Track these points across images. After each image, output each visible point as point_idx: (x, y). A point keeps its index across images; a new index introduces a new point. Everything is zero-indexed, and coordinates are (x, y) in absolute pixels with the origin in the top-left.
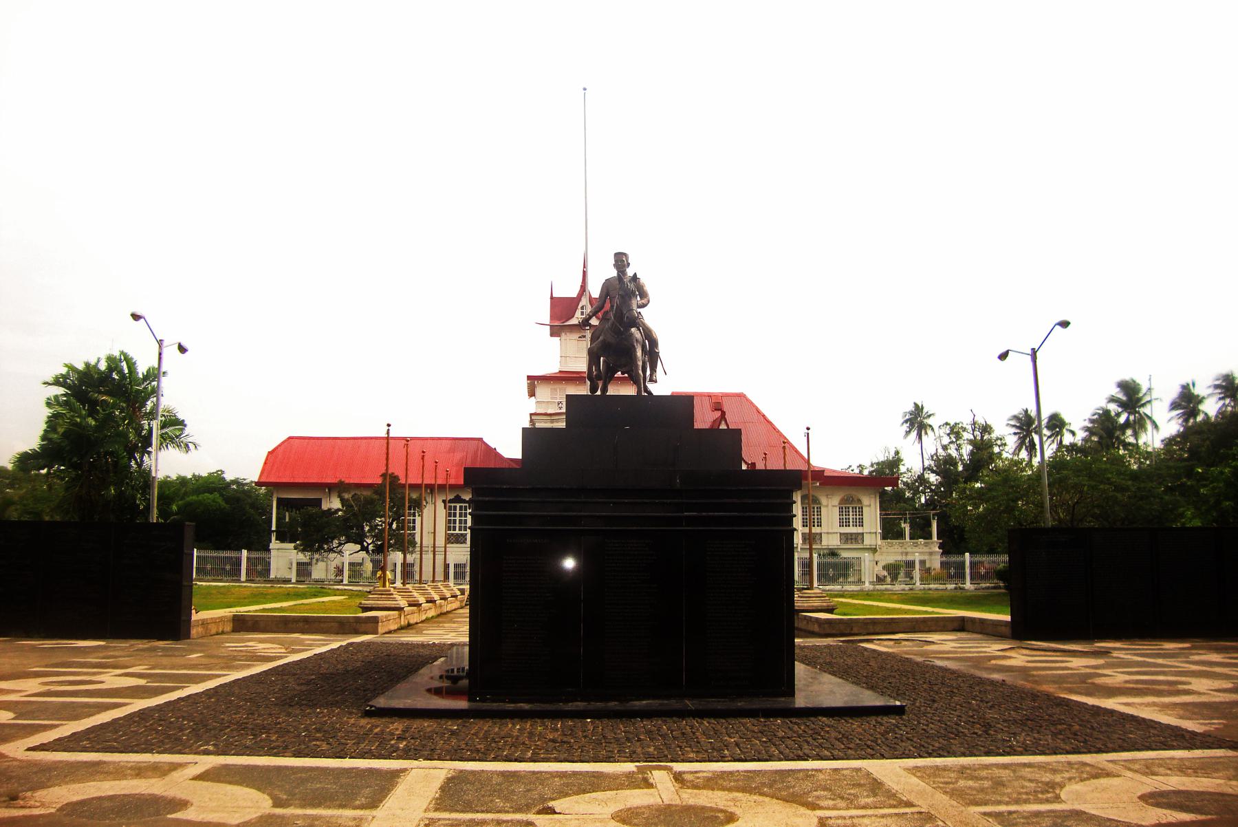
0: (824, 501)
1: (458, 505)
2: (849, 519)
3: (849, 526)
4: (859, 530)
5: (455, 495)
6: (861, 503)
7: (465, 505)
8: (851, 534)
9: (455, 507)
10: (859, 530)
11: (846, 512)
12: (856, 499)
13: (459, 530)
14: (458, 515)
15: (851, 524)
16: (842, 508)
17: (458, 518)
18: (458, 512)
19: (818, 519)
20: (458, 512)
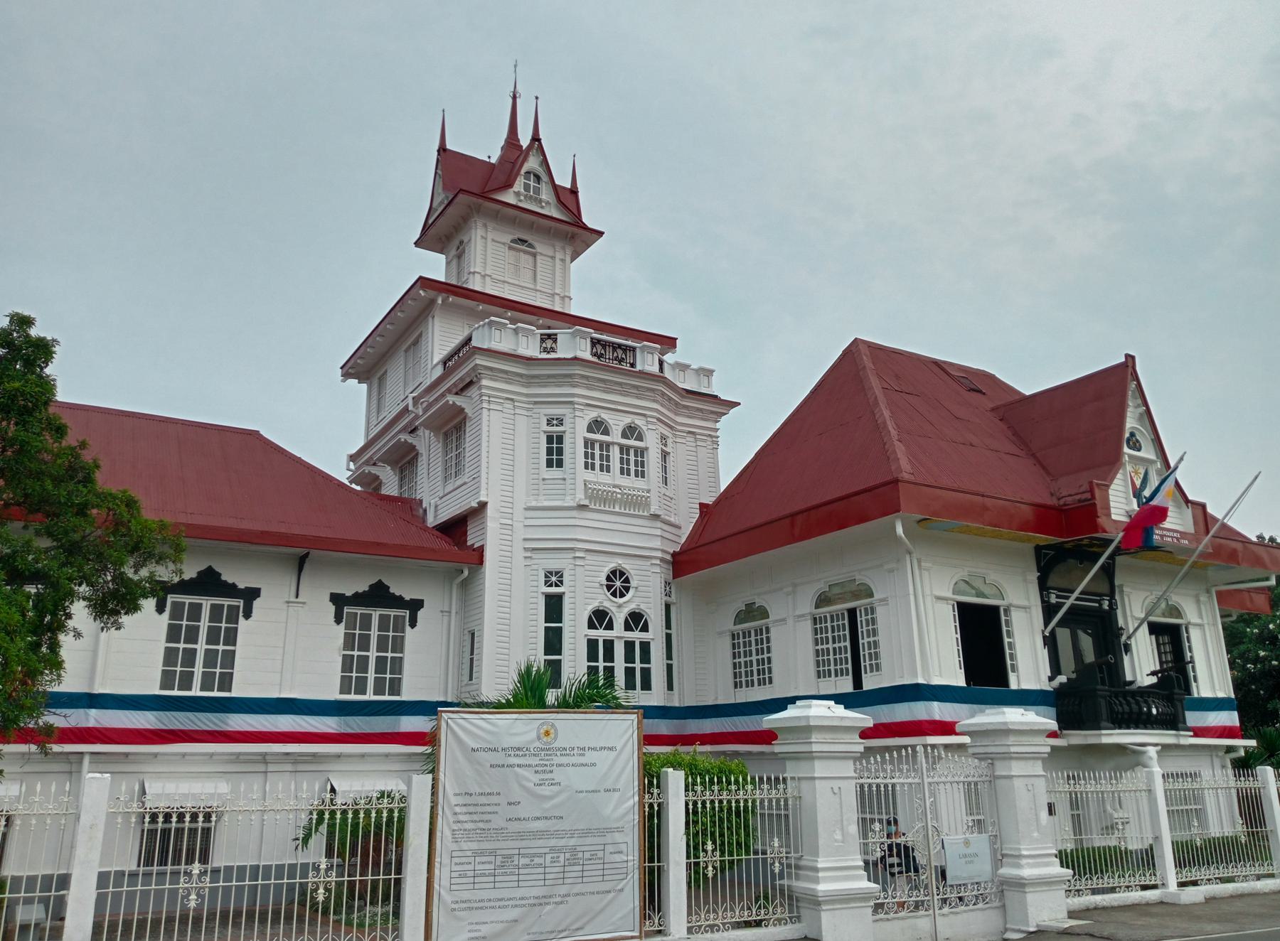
1: (207, 603)
5: (203, 567)
7: (234, 602)
9: (195, 612)
13: (202, 690)
17: (201, 647)
18: (204, 624)
20: (204, 624)
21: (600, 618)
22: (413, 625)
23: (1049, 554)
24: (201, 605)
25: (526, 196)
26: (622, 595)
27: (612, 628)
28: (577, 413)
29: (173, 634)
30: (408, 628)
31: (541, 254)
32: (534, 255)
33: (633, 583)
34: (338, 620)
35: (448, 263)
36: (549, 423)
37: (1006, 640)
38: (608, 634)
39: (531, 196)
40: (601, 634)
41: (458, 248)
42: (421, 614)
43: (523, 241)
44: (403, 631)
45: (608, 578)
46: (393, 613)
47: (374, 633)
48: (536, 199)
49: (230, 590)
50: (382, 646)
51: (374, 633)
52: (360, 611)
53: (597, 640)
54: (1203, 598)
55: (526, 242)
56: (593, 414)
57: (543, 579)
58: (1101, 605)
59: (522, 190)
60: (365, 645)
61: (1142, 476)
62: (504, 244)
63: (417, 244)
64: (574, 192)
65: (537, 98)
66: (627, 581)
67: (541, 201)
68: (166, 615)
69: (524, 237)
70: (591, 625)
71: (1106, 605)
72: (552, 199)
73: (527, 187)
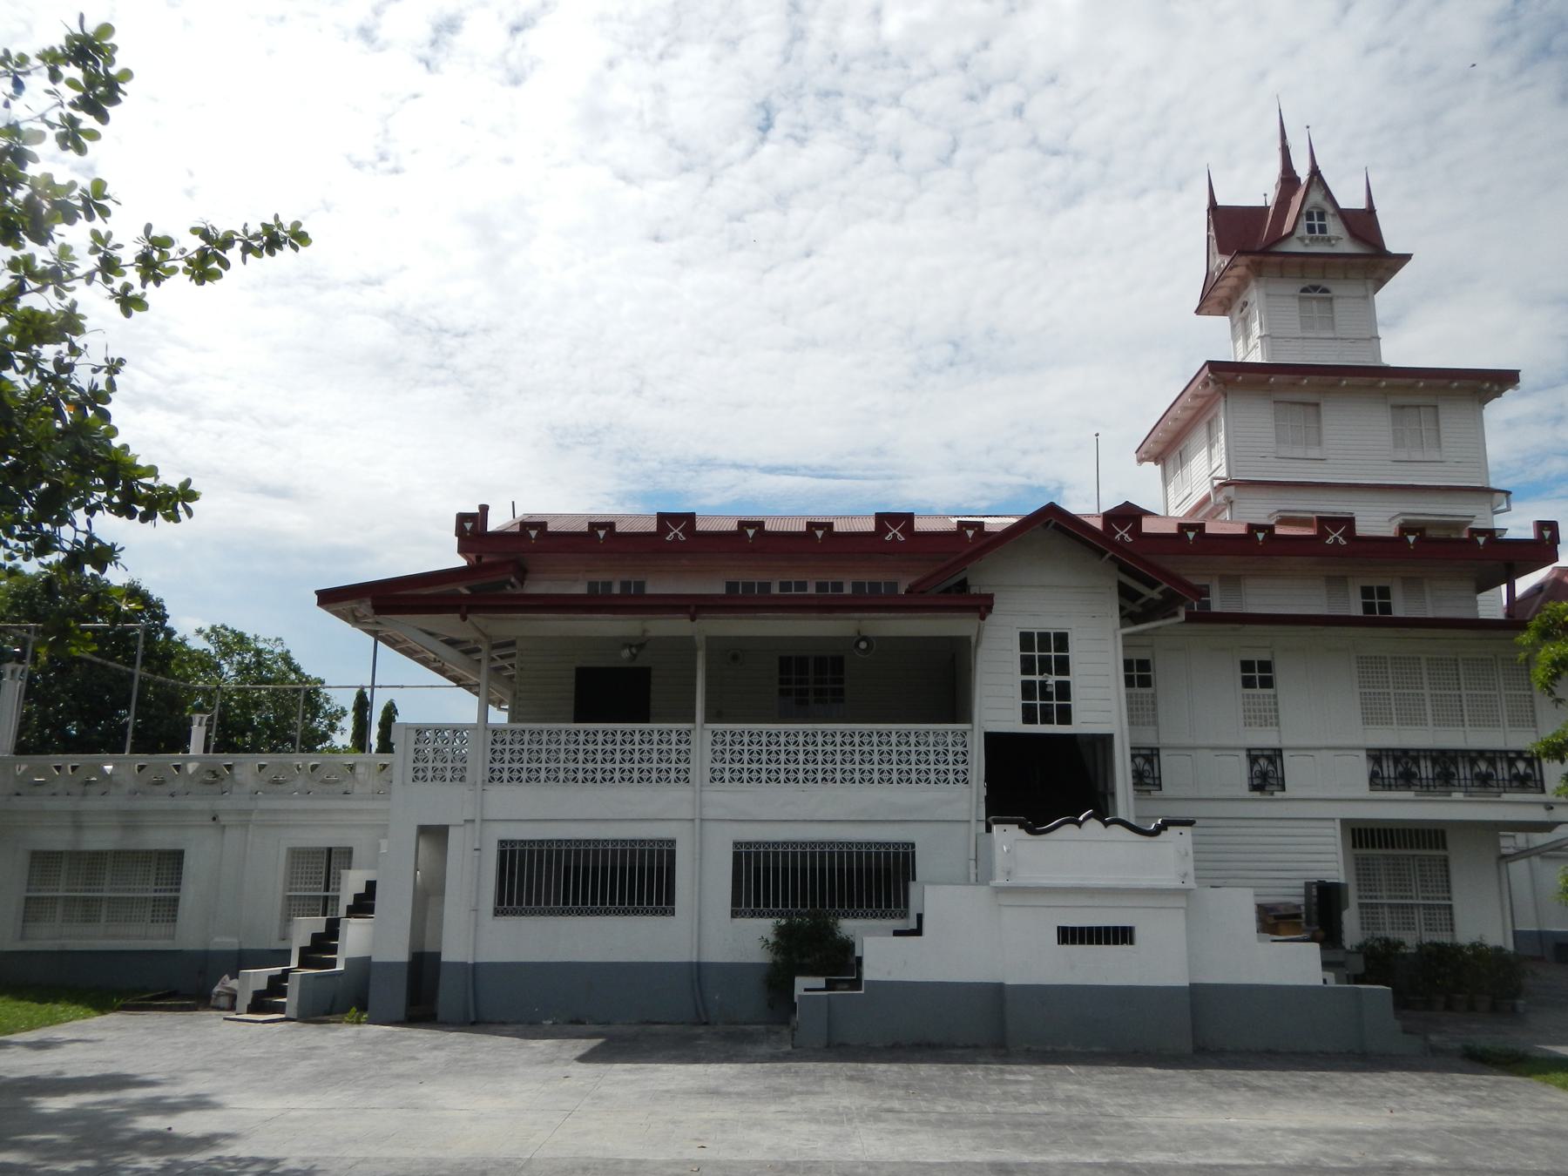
25: (1311, 239)
31: (1338, 297)
32: (1331, 299)
35: (1233, 327)
41: (1242, 311)
43: (1315, 288)
48: (1323, 239)
55: (1319, 287)
59: (1306, 233)
62: (1293, 296)
63: (1198, 311)
64: (1370, 211)
67: (1329, 240)
69: (1315, 283)
72: (1344, 234)
73: (1311, 229)
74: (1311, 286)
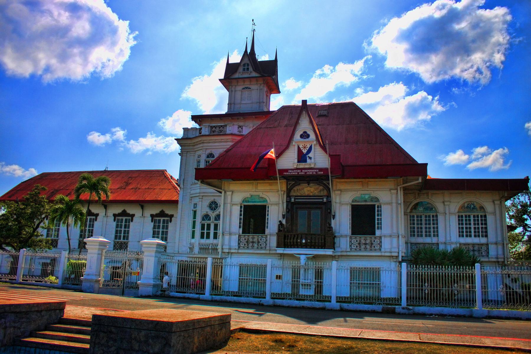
0: (440, 207)
1: (124, 218)
2: (470, 228)
3: (470, 236)
4: (483, 240)
5: (123, 210)
6: (485, 211)
8: (474, 245)
10: (483, 240)
11: (466, 220)
12: (477, 207)
14: (123, 227)
15: (473, 234)
16: (462, 216)
17: (123, 229)
19: (434, 228)
20: (123, 224)
21: (206, 217)
22: (171, 221)
23: (291, 183)
24: (123, 219)
26: (215, 209)
27: (210, 220)
28: (204, 152)
29: (117, 226)
30: (169, 223)
33: (218, 206)
34: (152, 222)
36: (198, 157)
37: (267, 217)
38: (209, 222)
39: (246, 72)
40: (206, 223)
42: (173, 219)
43: (247, 88)
44: (168, 224)
45: (210, 204)
46: (166, 219)
47: (161, 224)
49: (128, 215)
50: (163, 228)
51: (161, 224)
52: (158, 218)
53: (205, 224)
54: (395, 191)
56: (208, 152)
57: (192, 206)
58: (323, 200)
60: (159, 228)
61: (308, 149)
65: (247, 38)
66: (217, 204)
68: (116, 222)
70: (203, 219)
71: (325, 200)
73: (244, 70)
74: (245, 87)
